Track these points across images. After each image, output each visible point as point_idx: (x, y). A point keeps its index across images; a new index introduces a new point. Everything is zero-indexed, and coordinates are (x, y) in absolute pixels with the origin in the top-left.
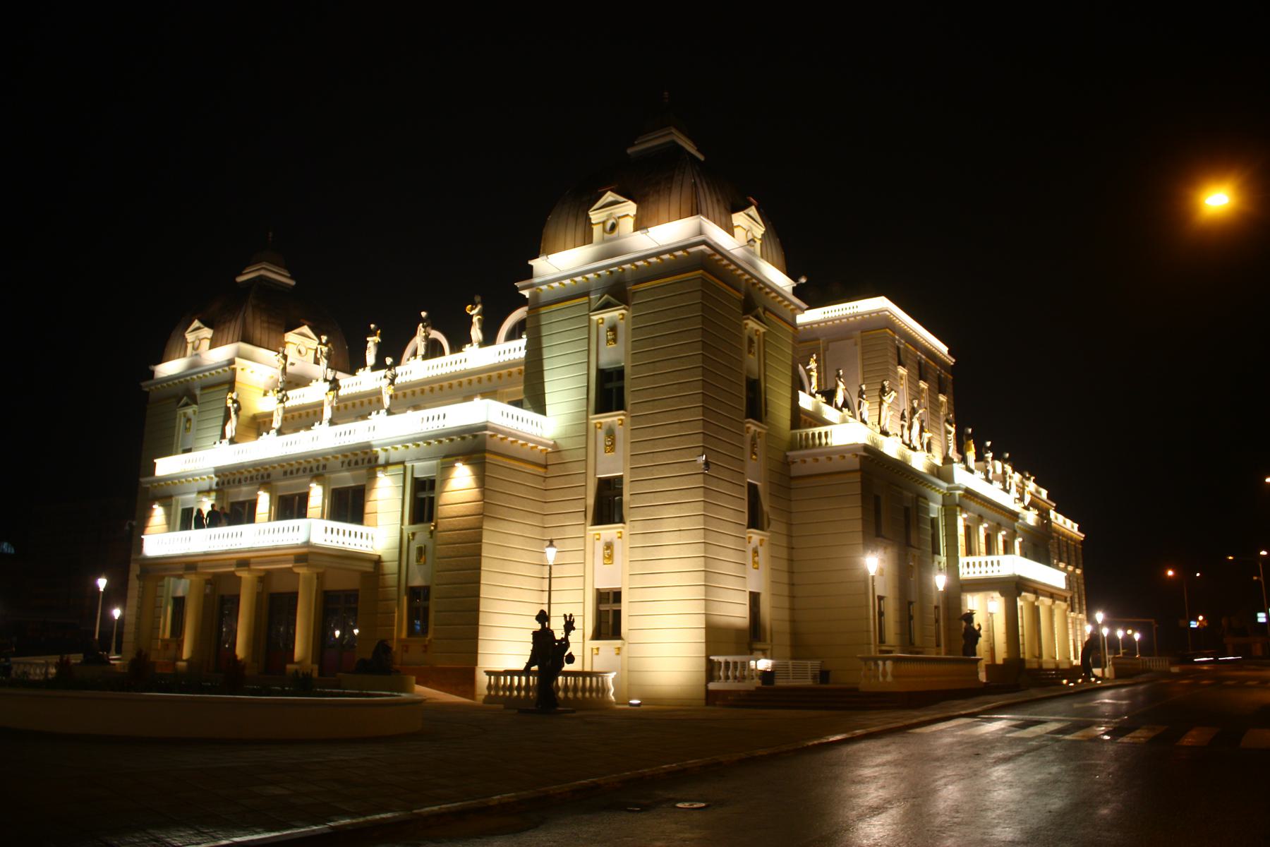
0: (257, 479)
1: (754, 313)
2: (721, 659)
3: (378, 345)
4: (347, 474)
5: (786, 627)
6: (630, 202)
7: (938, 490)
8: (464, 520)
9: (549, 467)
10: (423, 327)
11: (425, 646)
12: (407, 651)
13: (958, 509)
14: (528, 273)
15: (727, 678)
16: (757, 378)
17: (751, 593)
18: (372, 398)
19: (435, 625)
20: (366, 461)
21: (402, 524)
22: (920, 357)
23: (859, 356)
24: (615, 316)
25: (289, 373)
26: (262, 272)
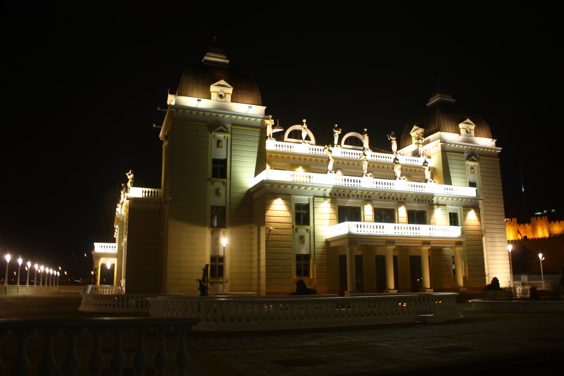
4: (416, 204)
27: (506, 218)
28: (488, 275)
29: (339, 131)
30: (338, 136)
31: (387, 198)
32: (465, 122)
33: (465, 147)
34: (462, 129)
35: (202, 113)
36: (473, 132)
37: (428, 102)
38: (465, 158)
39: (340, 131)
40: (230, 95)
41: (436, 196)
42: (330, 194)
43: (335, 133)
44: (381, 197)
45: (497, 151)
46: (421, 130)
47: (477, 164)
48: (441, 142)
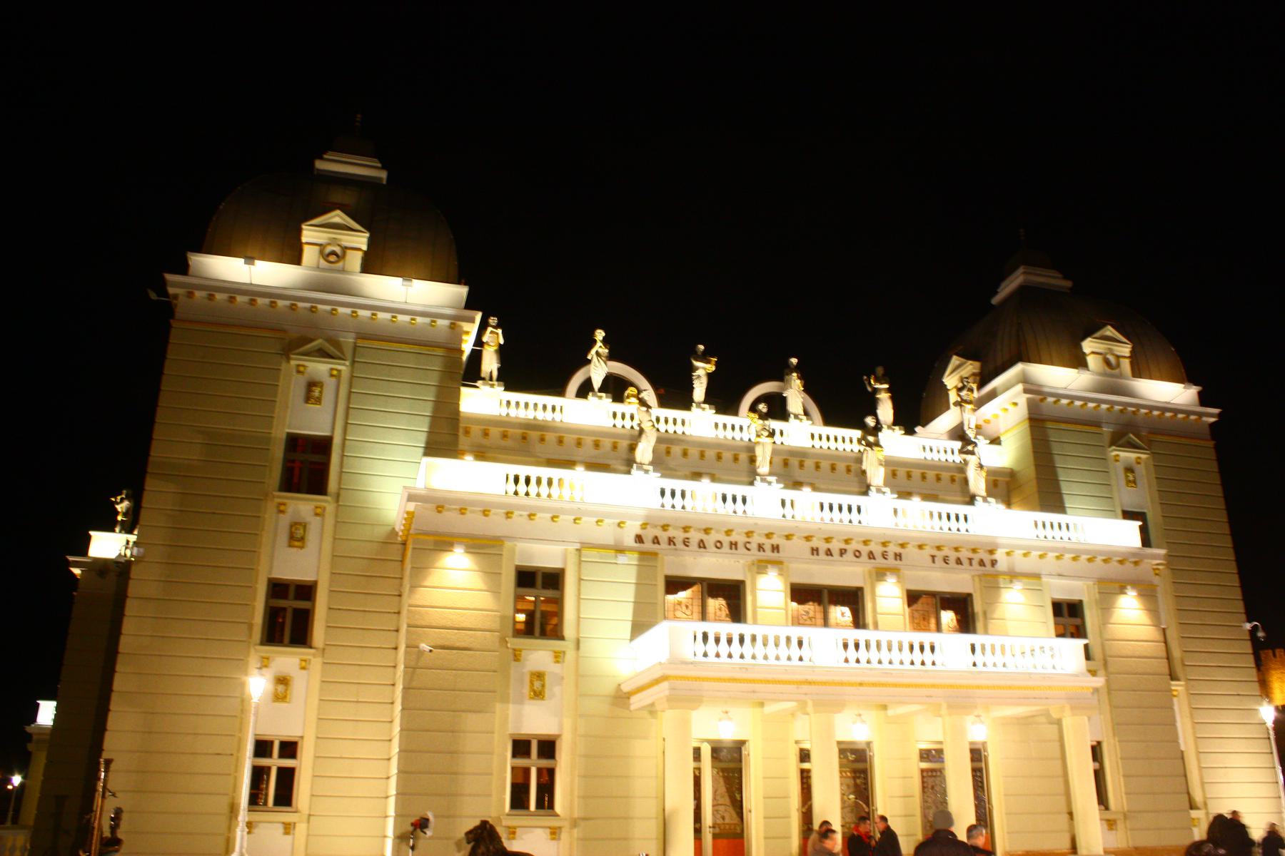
27: (1249, 621)
28: (1205, 804)
29: (708, 362)
30: (704, 381)
31: (836, 552)
32: (1098, 334)
33: (1104, 406)
34: (1092, 356)
35: (267, 301)
36: (1126, 365)
37: (996, 293)
38: (1107, 439)
39: (713, 363)
40: (359, 255)
41: (1004, 546)
42: (639, 539)
43: (697, 368)
44: (815, 551)
45: (1205, 419)
46: (971, 367)
47: (1144, 456)
48: (1026, 391)
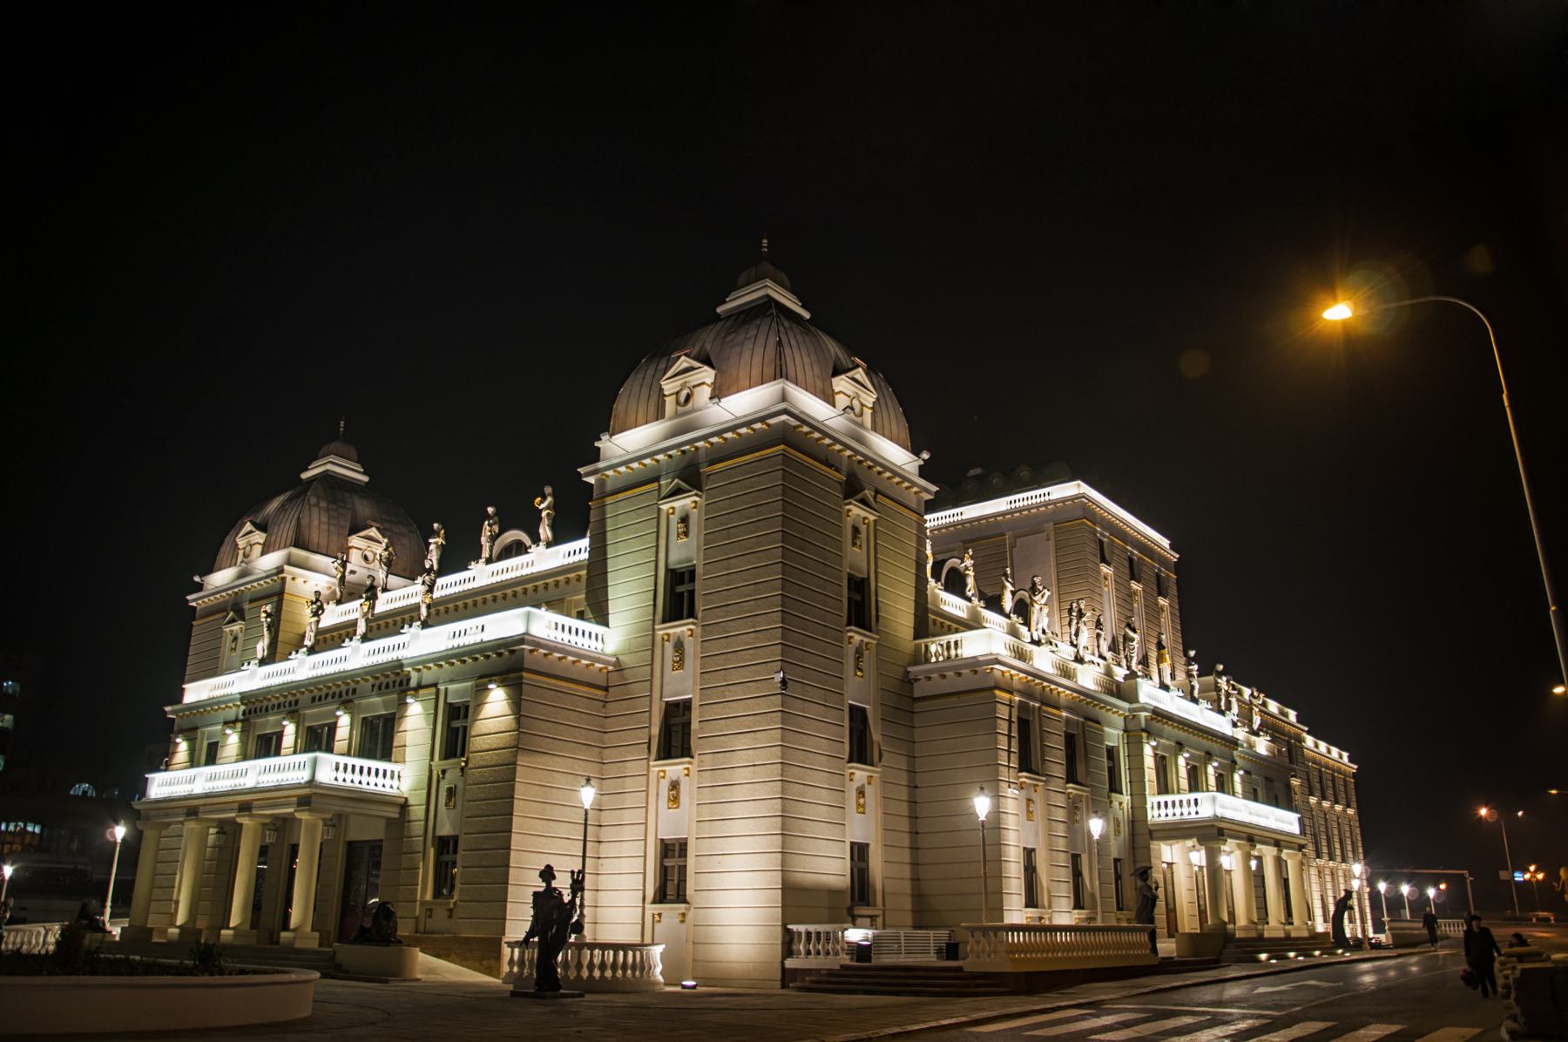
0: (285, 707)
1: (859, 496)
2: (802, 928)
3: (442, 548)
5: (907, 887)
6: (706, 368)
7: (1117, 712)
8: (497, 755)
9: (610, 689)
10: (490, 525)
11: (451, 910)
12: (430, 917)
13: (1144, 735)
14: (595, 455)
15: (808, 953)
16: (866, 576)
17: (853, 844)
18: (439, 608)
19: (462, 884)
20: (397, 683)
21: (432, 759)
22: (1132, 552)
23: (1052, 553)
24: (687, 504)
25: (349, 583)
26: (329, 467)
43: (430, 543)
45: (772, 421)
